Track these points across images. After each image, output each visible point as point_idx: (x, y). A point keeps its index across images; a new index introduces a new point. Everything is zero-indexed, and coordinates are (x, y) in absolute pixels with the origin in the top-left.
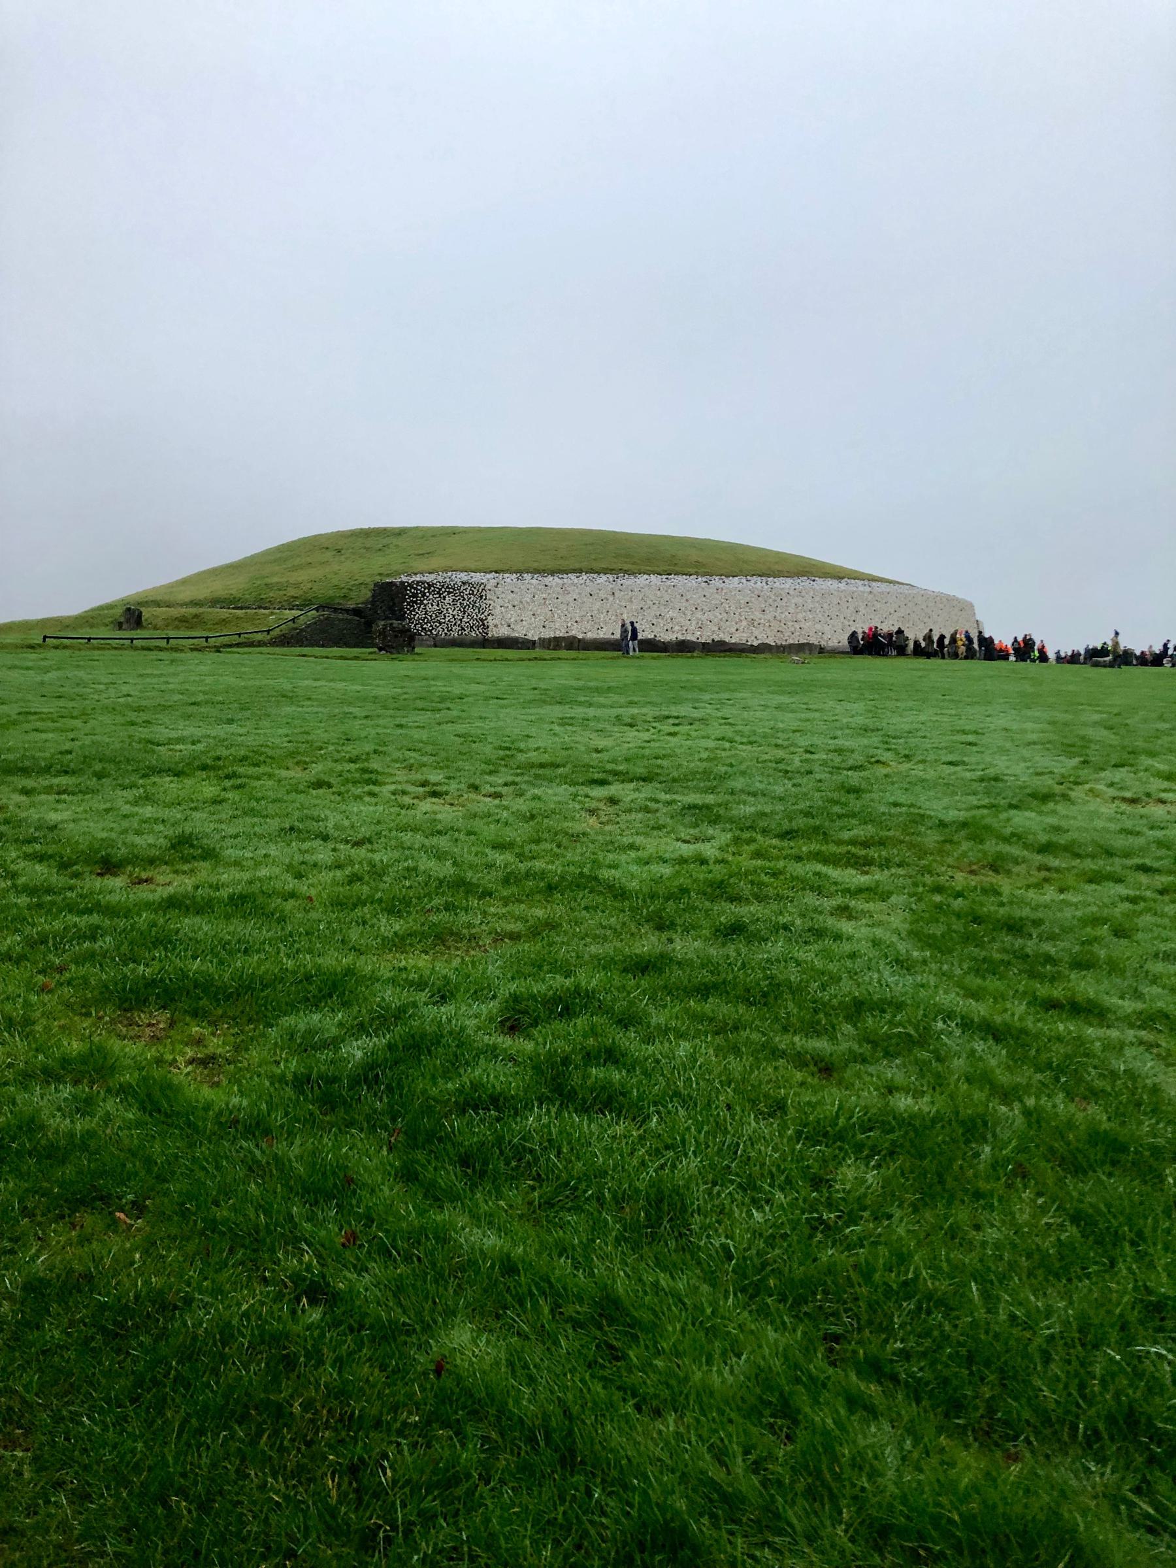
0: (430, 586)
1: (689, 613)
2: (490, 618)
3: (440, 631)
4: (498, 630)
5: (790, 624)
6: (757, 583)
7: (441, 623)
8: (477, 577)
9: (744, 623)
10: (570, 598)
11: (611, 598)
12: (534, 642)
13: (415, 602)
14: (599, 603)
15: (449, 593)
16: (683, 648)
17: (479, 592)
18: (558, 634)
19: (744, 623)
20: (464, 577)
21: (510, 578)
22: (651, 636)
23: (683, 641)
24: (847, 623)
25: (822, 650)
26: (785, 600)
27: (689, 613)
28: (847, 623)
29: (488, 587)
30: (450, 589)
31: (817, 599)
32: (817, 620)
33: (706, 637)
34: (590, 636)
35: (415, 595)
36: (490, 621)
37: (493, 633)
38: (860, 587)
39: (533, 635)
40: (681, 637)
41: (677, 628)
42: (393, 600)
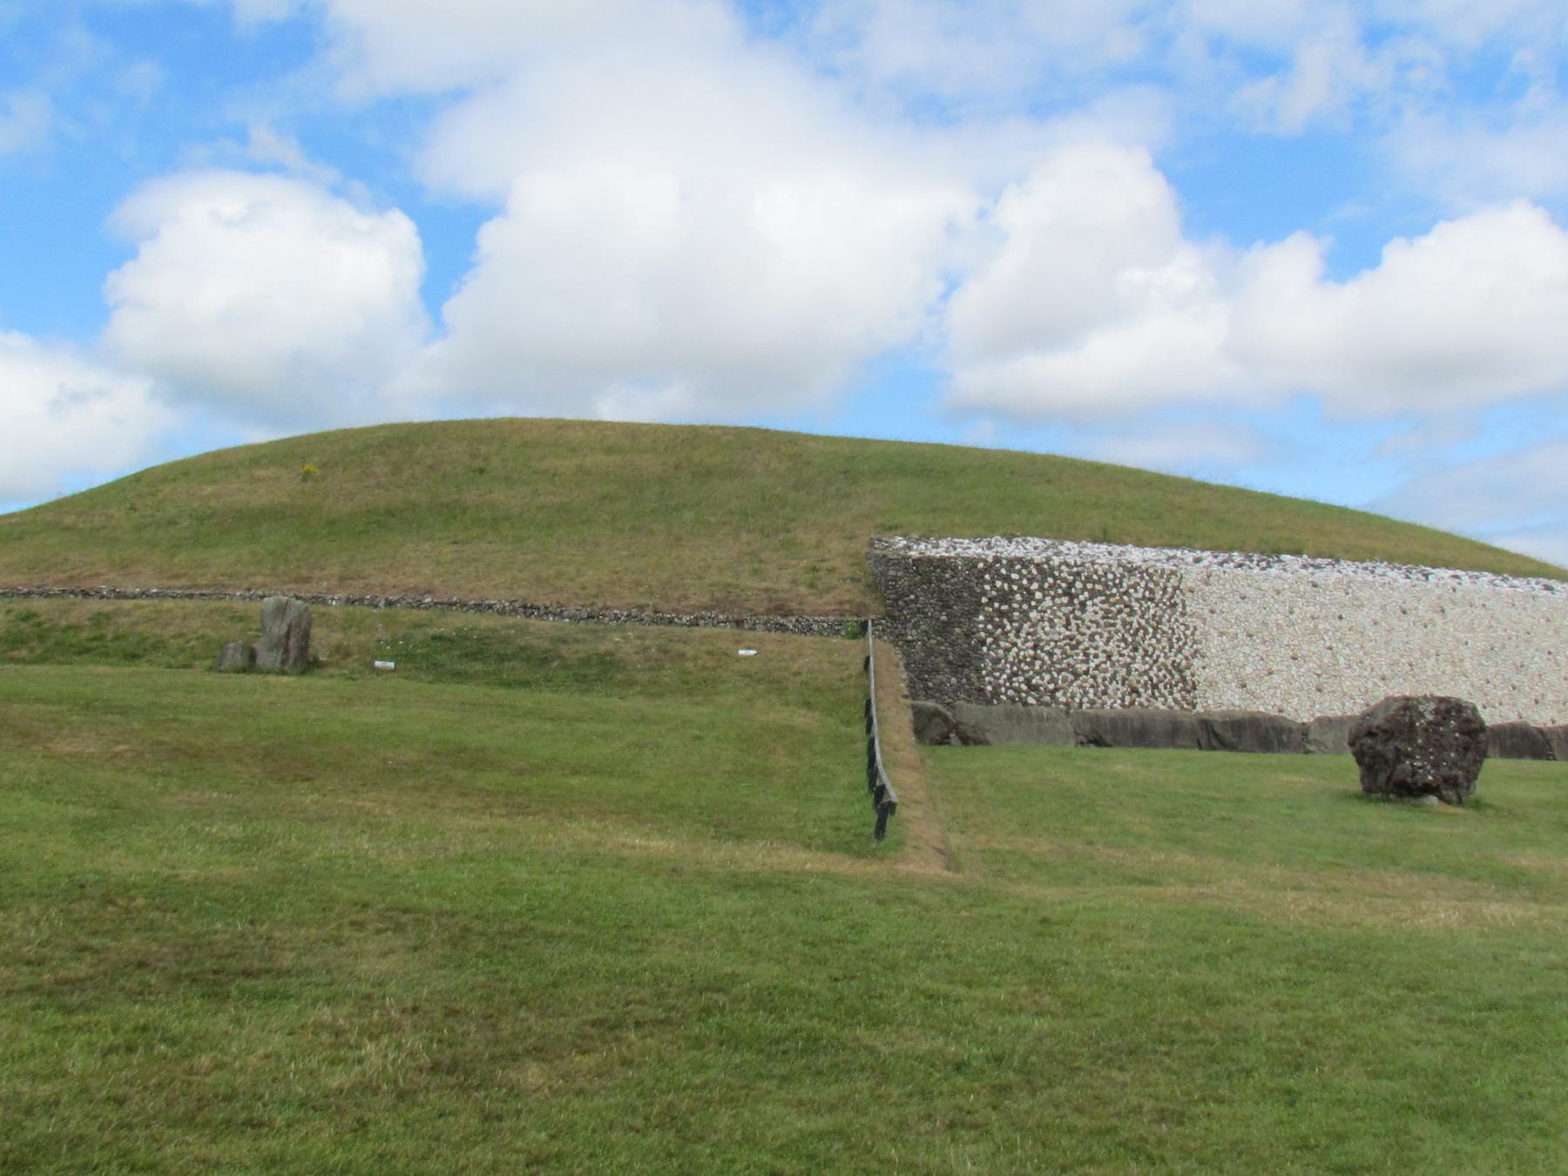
0: (1045, 571)
2: (1196, 662)
4: (1221, 697)
7: (1076, 675)
11: (1440, 622)
12: (1304, 730)
13: (1006, 614)
14: (1420, 632)
15: (1093, 594)
17: (1166, 595)
22: (1512, 718)
29: (1189, 582)
30: (1101, 585)
35: (1005, 597)
36: (1200, 671)
39: (1301, 711)
41: (1550, 697)
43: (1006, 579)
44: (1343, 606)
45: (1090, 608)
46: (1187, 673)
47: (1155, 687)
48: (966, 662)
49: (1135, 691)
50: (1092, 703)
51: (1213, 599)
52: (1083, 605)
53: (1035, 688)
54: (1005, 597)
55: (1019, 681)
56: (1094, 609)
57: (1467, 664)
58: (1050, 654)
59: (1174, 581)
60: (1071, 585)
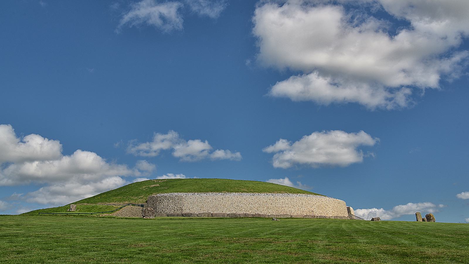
1: (247, 205)
2: (183, 207)
3: (168, 211)
6: (270, 196)
15: (171, 199)
17: (180, 198)
20: (176, 194)
21: (190, 194)
24: (299, 208)
27: (247, 205)
28: (299, 208)
30: (172, 198)
37: (184, 212)
40: (245, 213)
42: (153, 201)
43: (161, 198)
45: (170, 201)
46: (182, 208)
49: (175, 210)
50: (169, 212)
51: (186, 199)
52: (170, 200)
55: (161, 210)
57: (226, 206)
58: (165, 207)
59: (181, 197)
60: (168, 198)
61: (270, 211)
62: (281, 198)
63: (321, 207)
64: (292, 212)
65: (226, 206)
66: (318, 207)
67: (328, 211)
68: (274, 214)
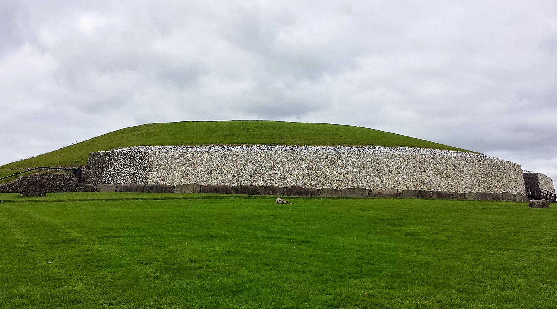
3: (122, 182)
4: (154, 180)
5: (348, 176)
6: (329, 150)
8: (143, 148)
9: (315, 175)
10: (197, 160)
12: (173, 188)
16: (271, 190)
17: (145, 157)
18: (189, 182)
19: (315, 175)
23: (270, 186)
25: (370, 195)
26: (345, 160)
30: (130, 156)
31: (369, 159)
32: (369, 172)
33: (287, 184)
34: (209, 183)
37: (151, 182)
38: (407, 151)
39: (174, 184)
40: (269, 184)
44: (191, 157)
47: (139, 179)
48: (100, 175)
53: (113, 180)
54: (110, 160)
56: (128, 162)
57: (232, 171)
61: (324, 181)
62: (350, 155)
63: (445, 175)
64: (374, 183)
65: (232, 171)
66: (437, 173)
67: (462, 183)
68: (333, 187)
